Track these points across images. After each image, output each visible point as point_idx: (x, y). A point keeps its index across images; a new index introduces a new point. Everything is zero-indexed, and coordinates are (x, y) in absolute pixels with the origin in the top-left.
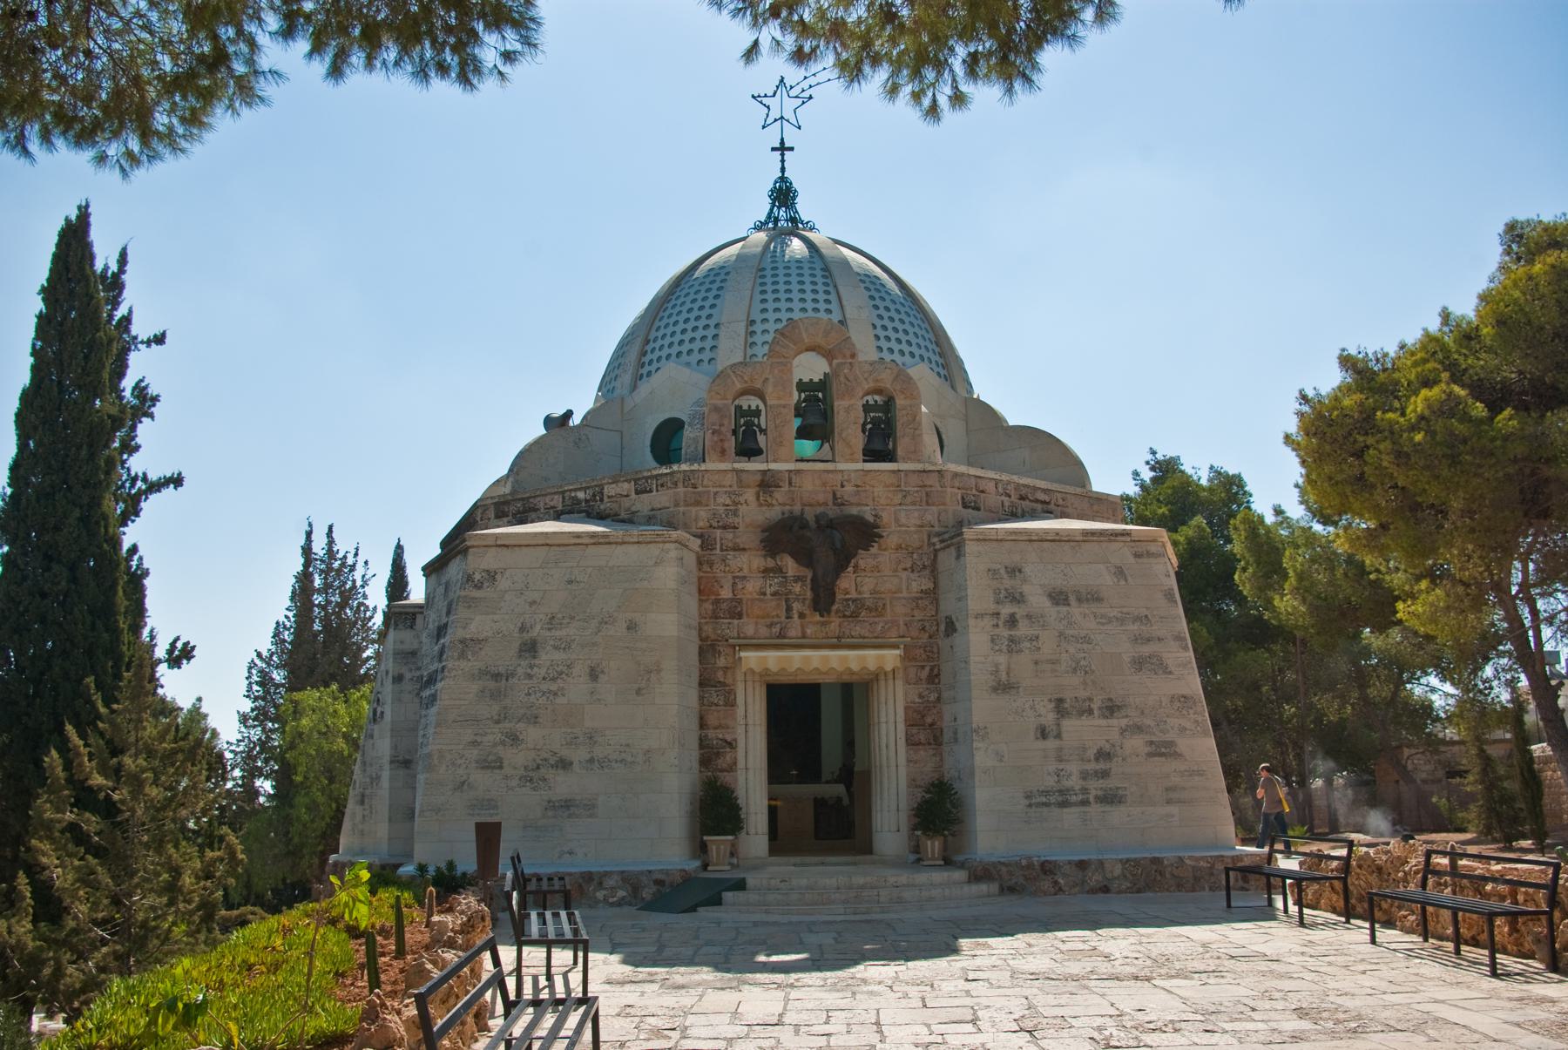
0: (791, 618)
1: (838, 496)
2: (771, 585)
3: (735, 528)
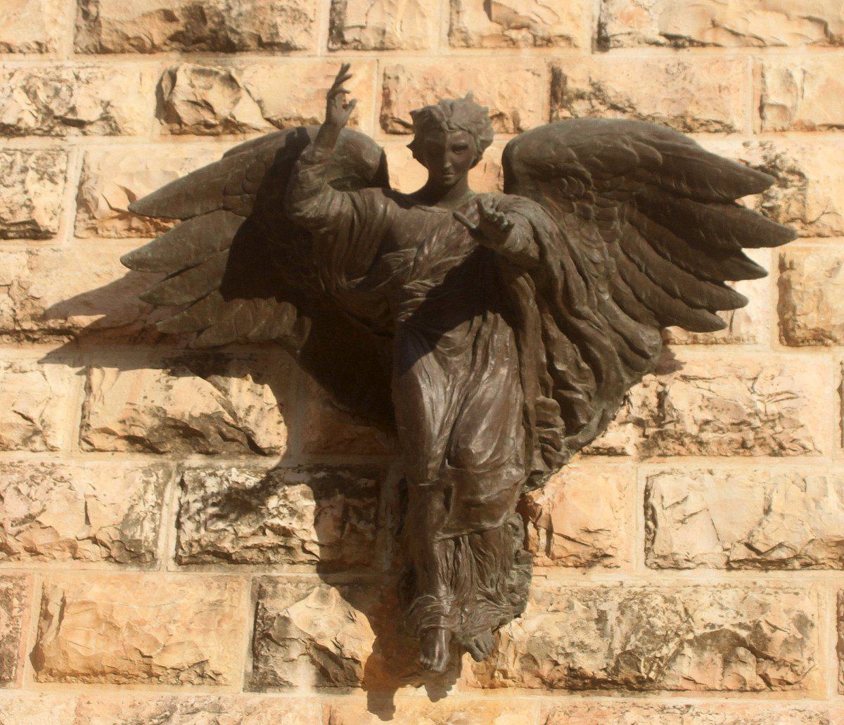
0: (278, 684)
1: (576, 81)
2: (183, 508)
3: (35, 233)
